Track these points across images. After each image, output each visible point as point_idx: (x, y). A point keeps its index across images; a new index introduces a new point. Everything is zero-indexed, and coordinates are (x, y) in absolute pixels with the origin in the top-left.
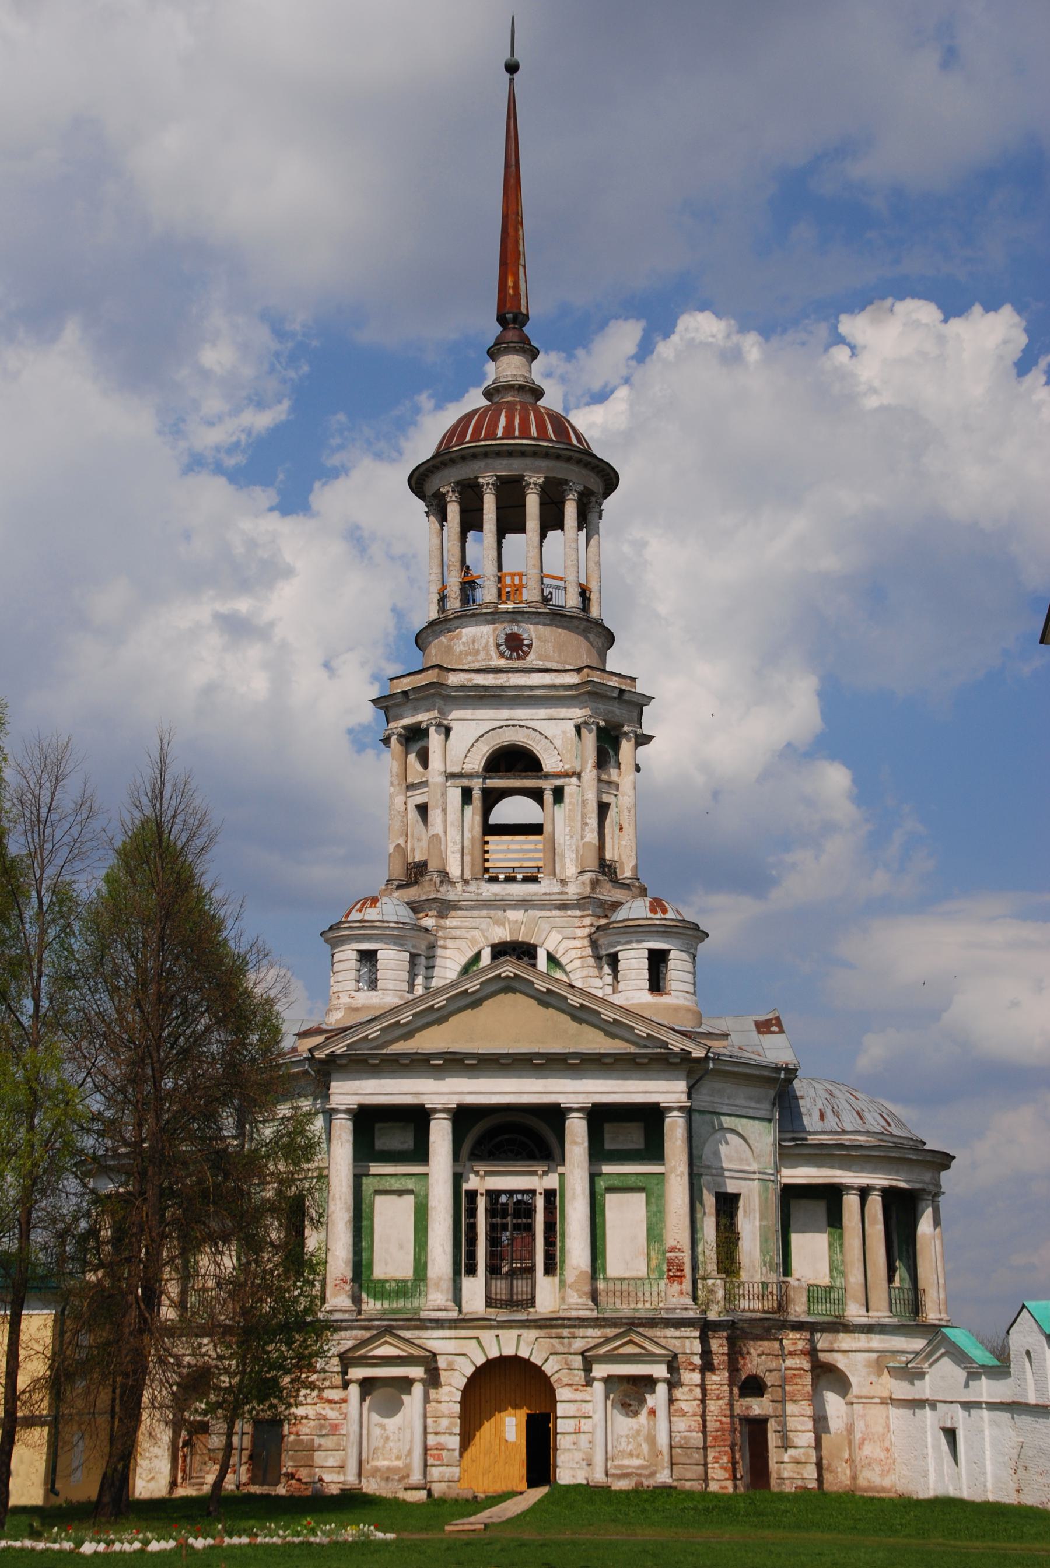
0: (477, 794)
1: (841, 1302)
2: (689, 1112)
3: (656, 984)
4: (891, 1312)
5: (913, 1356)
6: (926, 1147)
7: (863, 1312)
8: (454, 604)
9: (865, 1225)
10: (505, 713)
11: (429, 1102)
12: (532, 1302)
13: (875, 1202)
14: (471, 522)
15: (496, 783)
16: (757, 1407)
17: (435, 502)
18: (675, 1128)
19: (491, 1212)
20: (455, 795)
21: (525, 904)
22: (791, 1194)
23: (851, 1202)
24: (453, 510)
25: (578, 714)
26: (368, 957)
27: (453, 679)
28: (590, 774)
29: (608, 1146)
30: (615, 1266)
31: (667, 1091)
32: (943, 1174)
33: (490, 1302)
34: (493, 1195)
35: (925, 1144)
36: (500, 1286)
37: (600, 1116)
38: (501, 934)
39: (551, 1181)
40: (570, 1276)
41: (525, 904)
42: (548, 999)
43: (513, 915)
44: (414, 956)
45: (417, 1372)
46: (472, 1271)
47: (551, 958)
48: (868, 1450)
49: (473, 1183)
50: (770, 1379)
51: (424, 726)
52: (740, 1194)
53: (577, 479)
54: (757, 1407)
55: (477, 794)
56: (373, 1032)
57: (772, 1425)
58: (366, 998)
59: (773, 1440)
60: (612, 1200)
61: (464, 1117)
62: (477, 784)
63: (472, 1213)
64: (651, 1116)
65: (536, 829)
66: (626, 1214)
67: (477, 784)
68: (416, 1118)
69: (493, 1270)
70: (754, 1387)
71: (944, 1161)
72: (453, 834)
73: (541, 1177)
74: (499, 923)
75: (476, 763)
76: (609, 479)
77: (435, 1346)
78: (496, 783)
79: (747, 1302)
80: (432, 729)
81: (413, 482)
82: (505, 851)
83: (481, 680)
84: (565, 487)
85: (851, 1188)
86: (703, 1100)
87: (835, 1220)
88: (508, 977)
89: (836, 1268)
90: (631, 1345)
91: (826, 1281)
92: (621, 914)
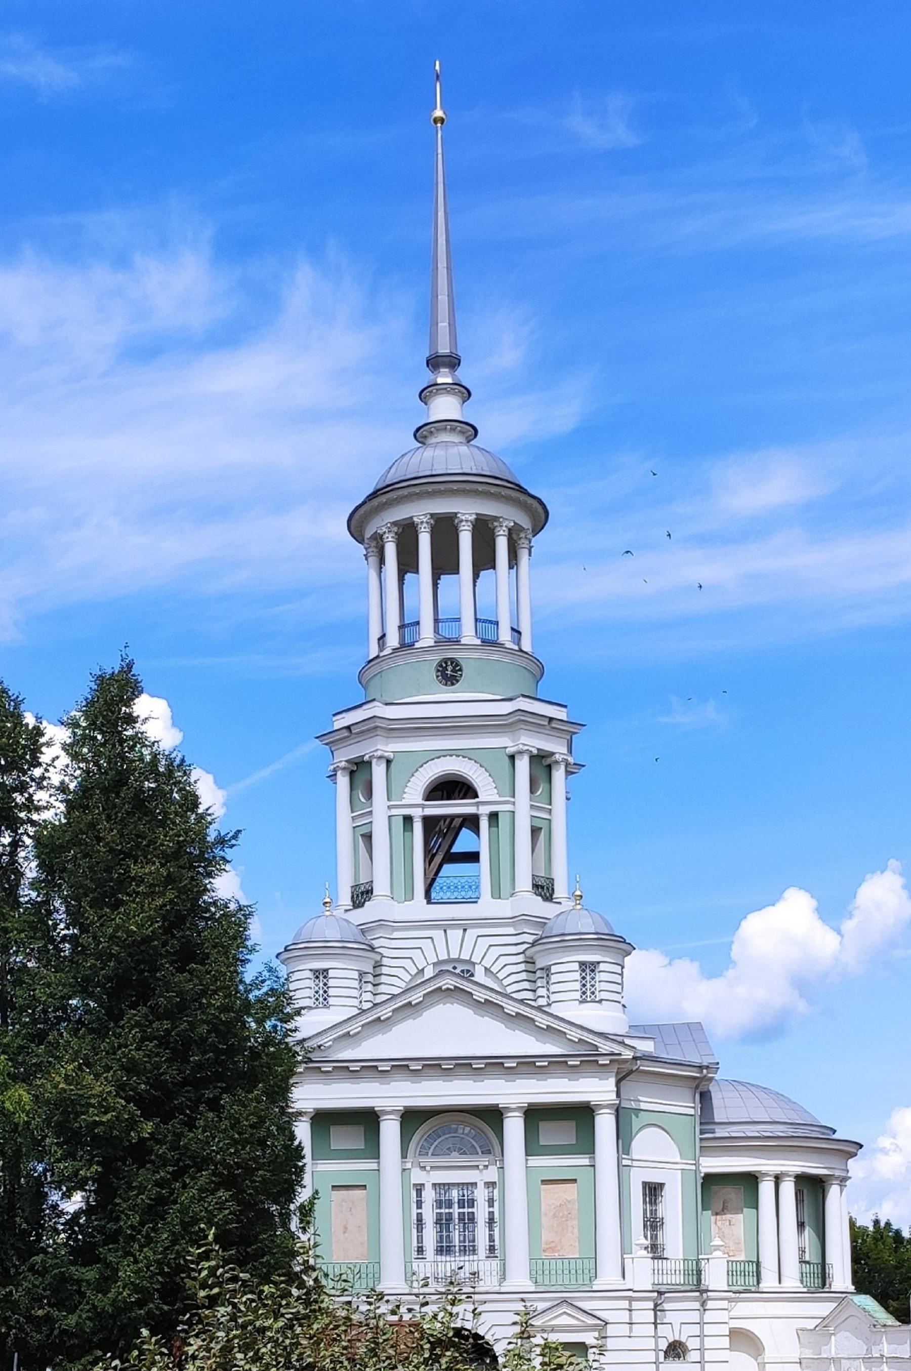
2: (618, 1111)
4: (802, 1283)
5: (820, 1320)
6: (835, 1136)
7: (778, 1285)
8: (393, 640)
9: (778, 1208)
11: (377, 1104)
13: (788, 1189)
14: (408, 563)
17: (374, 544)
18: (605, 1124)
22: (711, 1181)
23: (766, 1189)
24: (391, 550)
26: (321, 974)
31: (597, 1089)
32: (850, 1161)
35: (834, 1131)
37: (535, 1115)
39: (492, 1174)
42: (489, 1007)
49: (417, 1176)
51: (366, 758)
52: (662, 1185)
61: (412, 1118)
64: (582, 1115)
71: (850, 1149)
73: (481, 1171)
76: (540, 517)
79: (669, 1277)
80: (374, 761)
81: (353, 522)
84: (495, 524)
85: (766, 1175)
88: (448, 989)
90: (565, 1316)
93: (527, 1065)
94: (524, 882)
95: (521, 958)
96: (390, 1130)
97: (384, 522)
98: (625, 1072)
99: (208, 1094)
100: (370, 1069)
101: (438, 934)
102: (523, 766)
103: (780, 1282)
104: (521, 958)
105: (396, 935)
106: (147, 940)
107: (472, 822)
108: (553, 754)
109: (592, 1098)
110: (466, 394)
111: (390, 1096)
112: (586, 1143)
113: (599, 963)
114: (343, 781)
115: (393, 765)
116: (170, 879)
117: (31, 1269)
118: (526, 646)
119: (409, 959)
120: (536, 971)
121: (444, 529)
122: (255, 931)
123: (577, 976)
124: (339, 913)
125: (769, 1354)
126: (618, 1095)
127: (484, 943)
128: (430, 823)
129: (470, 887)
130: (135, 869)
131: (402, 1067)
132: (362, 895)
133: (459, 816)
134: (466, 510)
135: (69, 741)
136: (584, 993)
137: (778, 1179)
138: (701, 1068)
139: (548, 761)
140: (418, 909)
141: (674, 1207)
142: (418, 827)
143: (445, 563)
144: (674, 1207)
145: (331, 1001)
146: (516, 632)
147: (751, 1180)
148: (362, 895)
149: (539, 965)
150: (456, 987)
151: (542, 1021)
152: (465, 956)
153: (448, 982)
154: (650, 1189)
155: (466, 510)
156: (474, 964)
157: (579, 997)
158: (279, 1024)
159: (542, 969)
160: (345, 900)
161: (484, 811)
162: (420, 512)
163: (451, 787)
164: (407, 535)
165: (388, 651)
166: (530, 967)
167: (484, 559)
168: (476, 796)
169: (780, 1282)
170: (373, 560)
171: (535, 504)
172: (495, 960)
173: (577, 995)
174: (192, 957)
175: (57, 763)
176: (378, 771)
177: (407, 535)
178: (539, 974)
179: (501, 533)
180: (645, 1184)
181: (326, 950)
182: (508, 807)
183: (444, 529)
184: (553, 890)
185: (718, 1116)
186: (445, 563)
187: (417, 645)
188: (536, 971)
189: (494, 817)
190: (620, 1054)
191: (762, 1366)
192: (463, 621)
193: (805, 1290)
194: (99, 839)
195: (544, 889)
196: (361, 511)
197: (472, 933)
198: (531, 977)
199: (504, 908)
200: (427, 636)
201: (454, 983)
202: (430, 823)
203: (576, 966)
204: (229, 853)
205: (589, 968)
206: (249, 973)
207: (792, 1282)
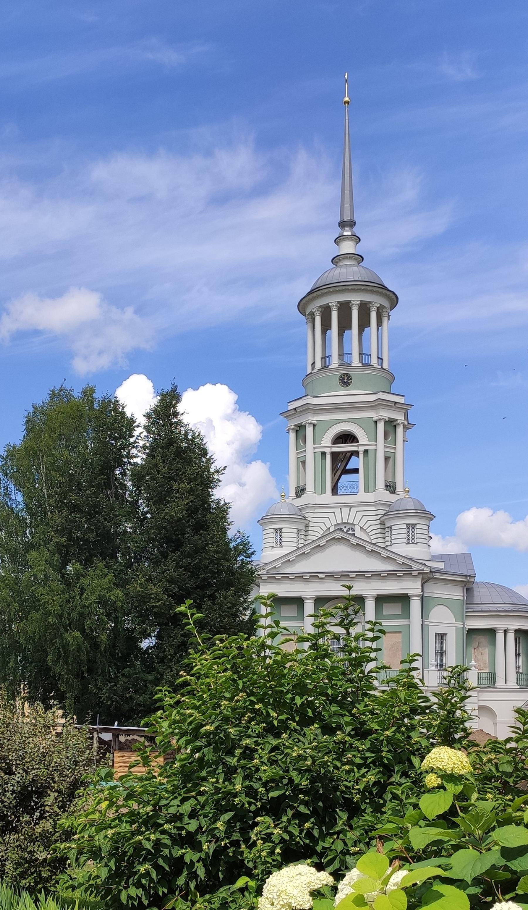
2: (422, 598)
7: (504, 684)
8: (318, 365)
13: (511, 636)
14: (326, 326)
17: (310, 317)
18: (415, 605)
23: (500, 636)
26: (279, 531)
31: (411, 587)
51: (303, 424)
56: (278, 564)
62: (328, 450)
64: (404, 599)
80: (307, 425)
84: (370, 305)
88: (338, 538)
93: (377, 575)
94: (381, 484)
95: (378, 522)
96: (309, 608)
97: (314, 306)
98: (427, 578)
99: (208, 593)
100: (299, 577)
101: (337, 511)
102: (381, 426)
103: (506, 683)
104: (378, 522)
105: (316, 511)
106: (180, 520)
107: (356, 453)
108: (397, 420)
109: (409, 592)
110: (358, 240)
112: (406, 614)
113: (416, 524)
114: (292, 436)
115: (316, 427)
116: (192, 490)
117: (123, 675)
118: (385, 366)
119: (322, 523)
120: (385, 528)
121: (345, 309)
122: (232, 516)
123: (405, 531)
124: (289, 500)
125: (498, 719)
126: (423, 590)
127: (360, 515)
128: (335, 456)
129: (354, 487)
130: (175, 486)
131: (315, 576)
132: (300, 491)
133: (349, 452)
134: (355, 299)
135: (147, 425)
136: (409, 539)
137: (506, 632)
138: (466, 576)
139: (395, 423)
140: (328, 497)
141: (451, 646)
142: (328, 458)
143: (345, 325)
144: (451, 646)
145: (283, 544)
146: (380, 359)
147: (492, 632)
148: (300, 491)
149: (386, 526)
150: (342, 537)
151: (384, 554)
152: (350, 521)
153: (338, 535)
154: (439, 636)
156: (355, 525)
157: (406, 542)
158: (245, 558)
159: (388, 527)
160: (293, 494)
161: (361, 449)
162: (333, 301)
163: (347, 437)
164: (326, 312)
165: (316, 370)
166: (383, 526)
168: (358, 442)
169: (506, 683)
170: (310, 325)
171: (391, 295)
172: (366, 524)
173: (405, 541)
174: (202, 528)
175: (141, 436)
176: (309, 430)
177: (326, 312)
178: (387, 530)
179: (373, 310)
180: (436, 634)
181: (281, 520)
182: (373, 447)
183: (345, 309)
184: (396, 488)
185: (477, 600)
186: (345, 325)
187: (330, 367)
188: (385, 528)
189: (366, 452)
190: (423, 570)
191: (495, 724)
192: (353, 354)
193: (519, 687)
194: (159, 472)
195: (391, 488)
196: (304, 301)
197: (354, 510)
198: (383, 531)
199: (370, 497)
200: (335, 362)
201: (343, 535)
202: (335, 456)
203: (405, 526)
204: (221, 477)
206: (230, 534)
207: (512, 683)
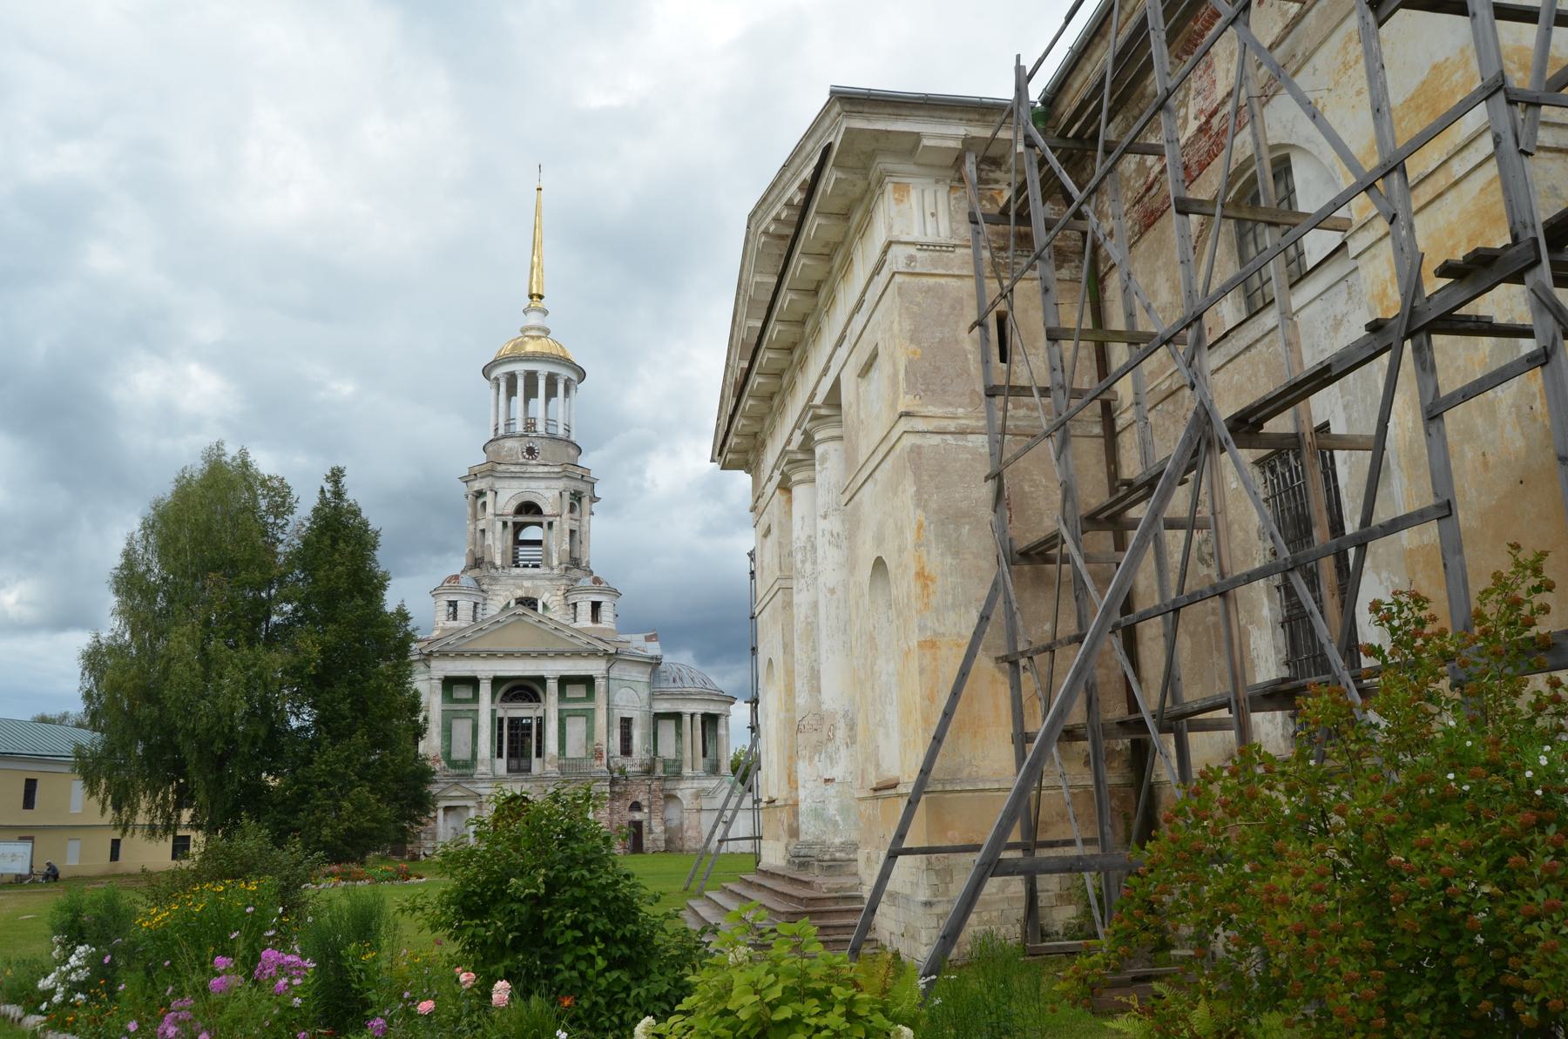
0: (510, 524)
1: (680, 767)
3: (595, 616)
10: (525, 484)
12: (529, 770)
13: (698, 719)
14: (511, 391)
15: (521, 519)
16: (638, 816)
18: (600, 684)
19: (510, 728)
20: (499, 525)
21: (532, 577)
22: (658, 717)
23: (687, 719)
25: (561, 484)
27: (500, 468)
28: (566, 515)
29: (568, 695)
30: (570, 753)
33: (509, 770)
34: (512, 720)
36: (514, 762)
37: (564, 681)
38: (520, 593)
39: (540, 713)
40: (547, 758)
41: (532, 577)
43: (527, 584)
44: (476, 604)
45: (470, 803)
46: (500, 755)
47: (545, 606)
48: (690, 833)
49: (500, 713)
50: (645, 803)
53: (564, 373)
54: (638, 816)
55: (510, 524)
57: (645, 824)
58: (452, 624)
59: (645, 830)
60: (569, 721)
61: (497, 682)
63: (501, 728)
64: (588, 681)
65: (538, 543)
66: (576, 728)
67: (510, 520)
68: (473, 682)
69: (510, 755)
70: (636, 806)
72: (499, 545)
74: (520, 587)
75: (511, 508)
77: (481, 791)
78: (521, 519)
82: (524, 551)
83: (513, 468)
86: (614, 673)
87: (679, 726)
89: (679, 751)
91: (673, 757)
92: (580, 584)
96: (485, 690)
97: (499, 372)
111: (485, 669)
121: (531, 377)
143: (531, 392)
155: (543, 370)
162: (520, 368)
167: (551, 392)
170: (493, 392)
183: (531, 377)
200: (519, 428)
202: (515, 524)
205: (596, 606)
